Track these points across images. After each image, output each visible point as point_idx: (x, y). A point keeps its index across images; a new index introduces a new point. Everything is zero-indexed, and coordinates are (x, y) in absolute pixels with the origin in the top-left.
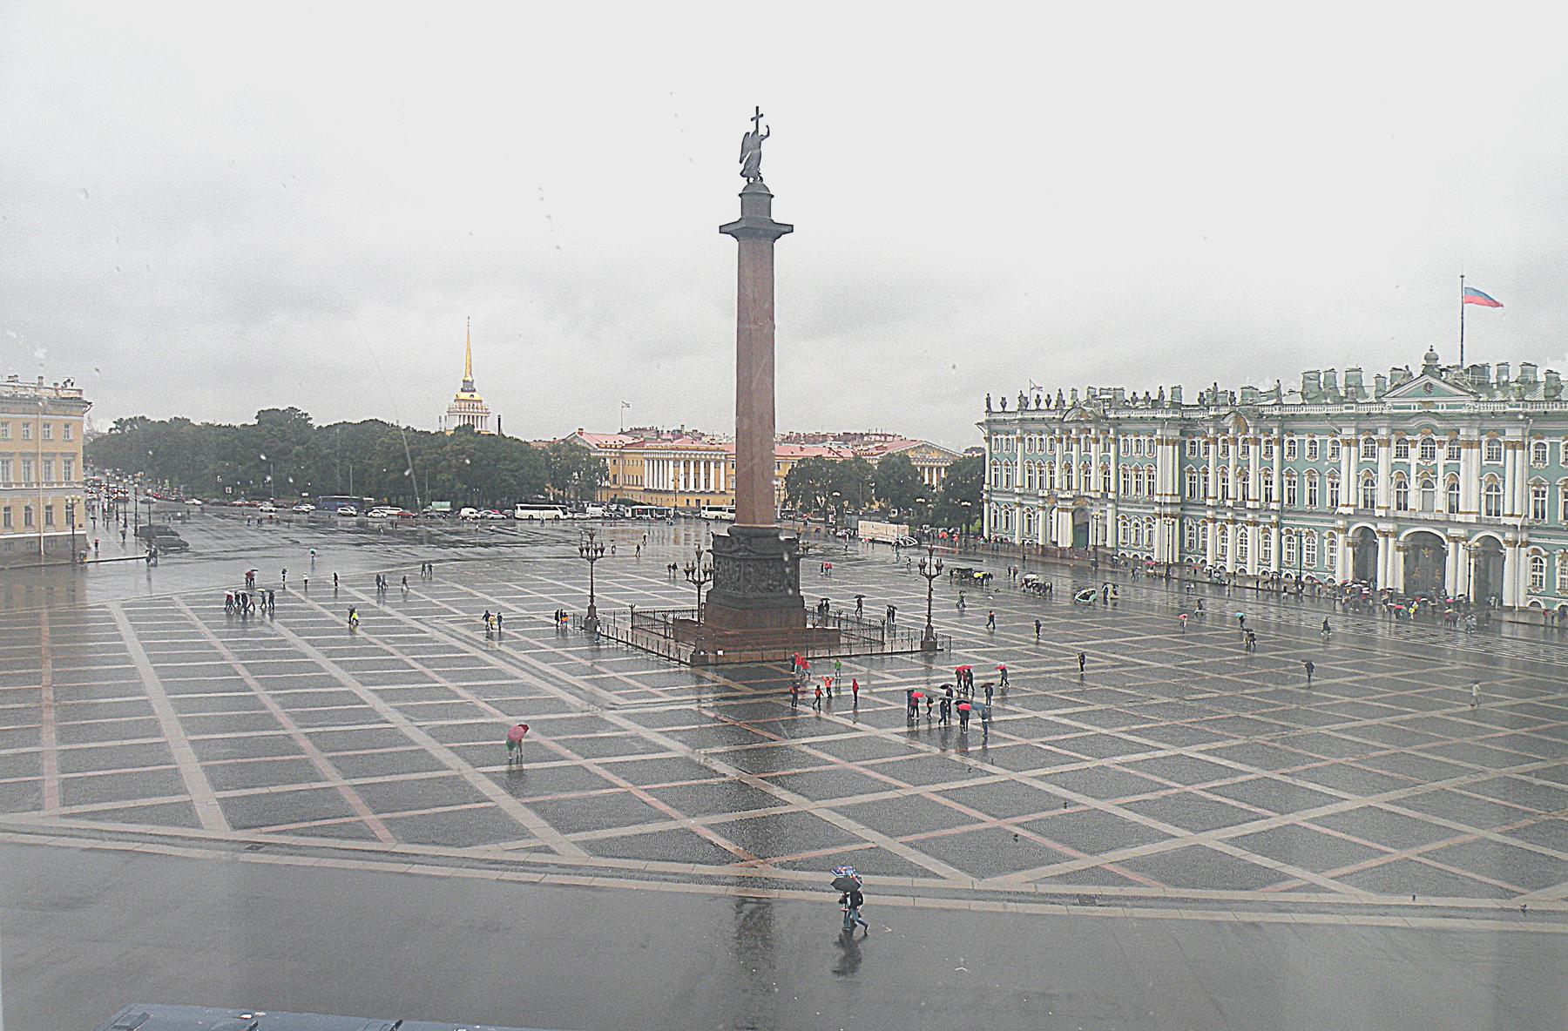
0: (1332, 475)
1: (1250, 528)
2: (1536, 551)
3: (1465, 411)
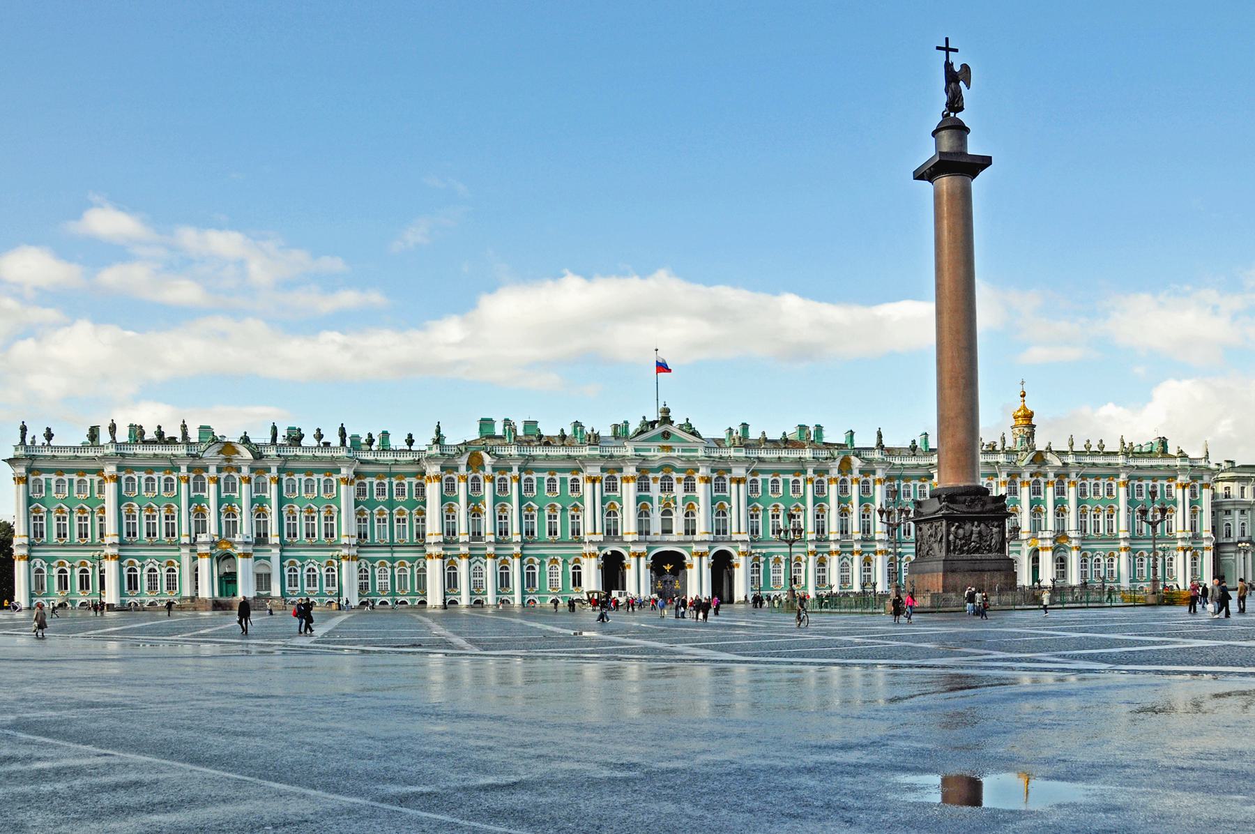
1: (489, 560)
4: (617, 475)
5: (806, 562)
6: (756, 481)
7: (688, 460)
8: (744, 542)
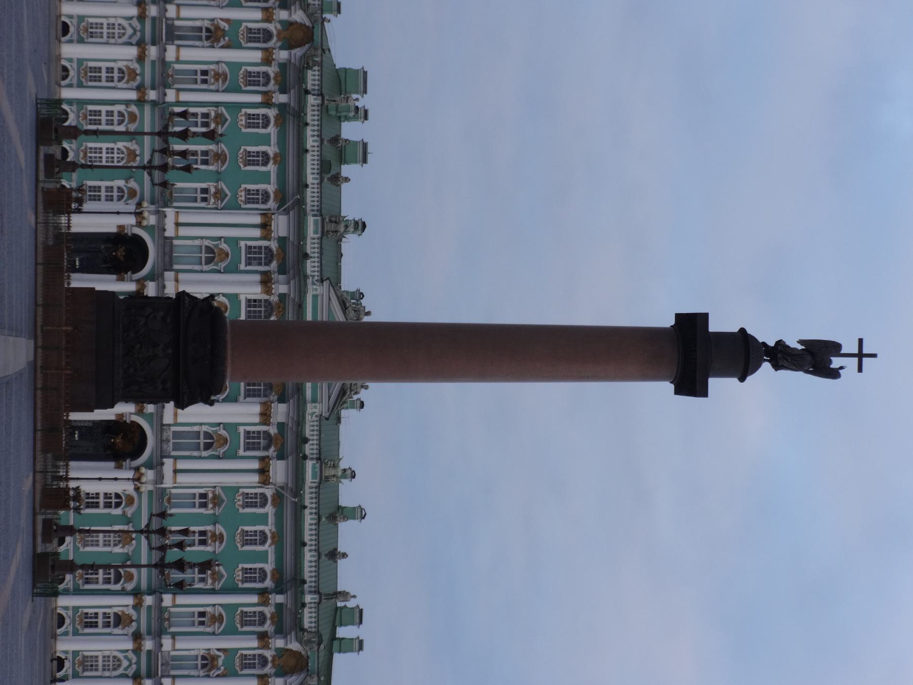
0: (219, 195)
1: (133, 51)
2: (130, 500)
3: (310, 408)
4: (274, 265)
5: (123, 592)
6: (263, 505)
7: (300, 390)
8: (160, 478)
